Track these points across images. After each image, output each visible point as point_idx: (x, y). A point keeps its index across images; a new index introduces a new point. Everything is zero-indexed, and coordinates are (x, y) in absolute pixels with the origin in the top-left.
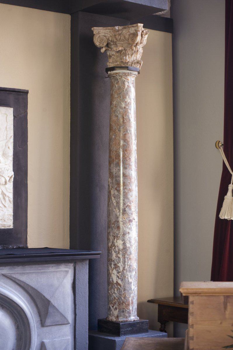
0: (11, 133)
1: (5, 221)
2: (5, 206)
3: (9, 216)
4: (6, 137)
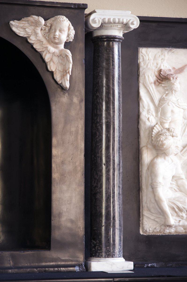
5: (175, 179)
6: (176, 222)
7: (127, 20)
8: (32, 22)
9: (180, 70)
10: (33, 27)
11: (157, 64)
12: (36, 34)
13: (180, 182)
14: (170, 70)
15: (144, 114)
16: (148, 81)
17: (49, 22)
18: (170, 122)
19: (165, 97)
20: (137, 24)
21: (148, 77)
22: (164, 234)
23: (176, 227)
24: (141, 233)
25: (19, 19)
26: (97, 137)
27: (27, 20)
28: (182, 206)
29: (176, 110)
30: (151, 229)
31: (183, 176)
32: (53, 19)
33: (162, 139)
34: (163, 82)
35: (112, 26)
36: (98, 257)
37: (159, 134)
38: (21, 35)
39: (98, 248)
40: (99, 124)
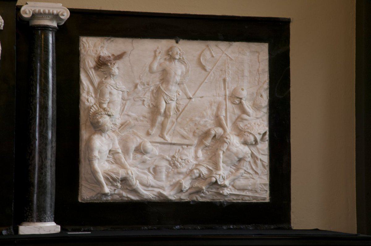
0: (266, 77)
1: (256, 192)
2: (256, 173)
3: (262, 186)
4: (258, 83)
5: (111, 153)
6: (111, 190)
7: (57, 11)
9: (119, 57)
11: (97, 51)
13: (116, 156)
14: (109, 57)
15: (84, 95)
16: (88, 66)
18: (108, 103)
19: (104, 80)
20: (67, 15)
21: (88, 62)
22: (101, 202)
23: (111, 195)
24: (80, 200)
26: (30, 115)
28: (116, 177)
29: (115, 92)
30: (88, 197)
31: (120, 151)
33: (97, 117)
34: (102, 67)
35: (43, 16)
36: (29, 222)
37: (96, 113)
39: (28, 214)
40: (32, 103)
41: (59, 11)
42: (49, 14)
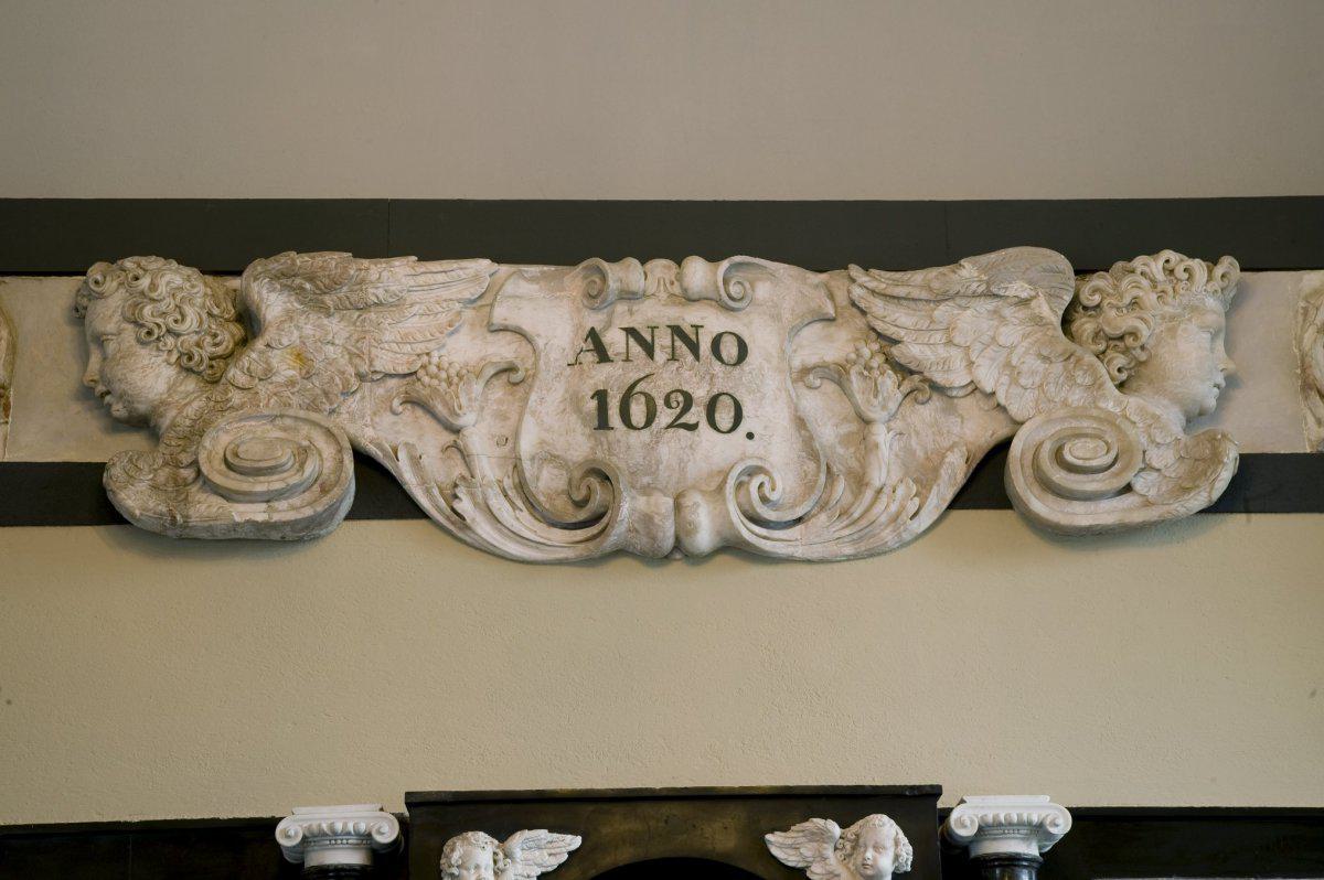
8: (813, 833)
10: (815, 844)
12: (824, 859)
17: (854, 828)
25: (785, 829)
27: (801, 828)
32: (860, 822)
38: (790, 864)
41: (1043, 815)
42: (1021, 824)
